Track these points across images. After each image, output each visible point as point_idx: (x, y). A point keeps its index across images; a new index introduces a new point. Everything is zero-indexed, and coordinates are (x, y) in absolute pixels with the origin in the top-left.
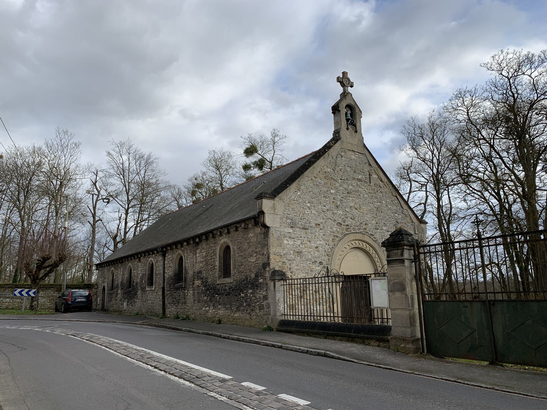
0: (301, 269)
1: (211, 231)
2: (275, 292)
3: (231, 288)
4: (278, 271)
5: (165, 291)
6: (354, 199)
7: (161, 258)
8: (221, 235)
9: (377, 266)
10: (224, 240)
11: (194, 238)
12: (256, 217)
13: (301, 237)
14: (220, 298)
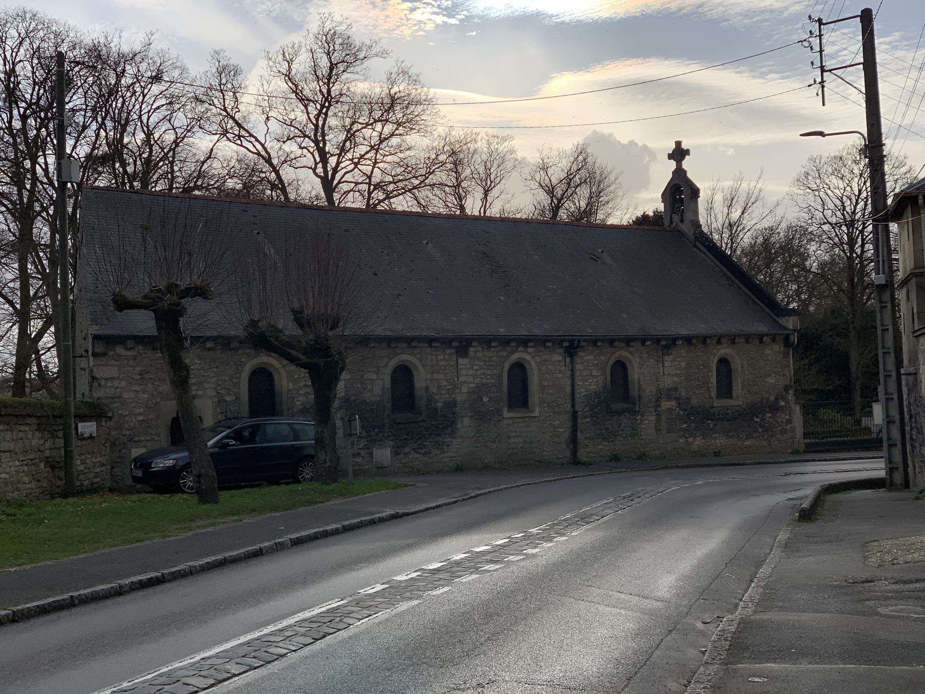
3: (737, 411)
10: (724, 350)
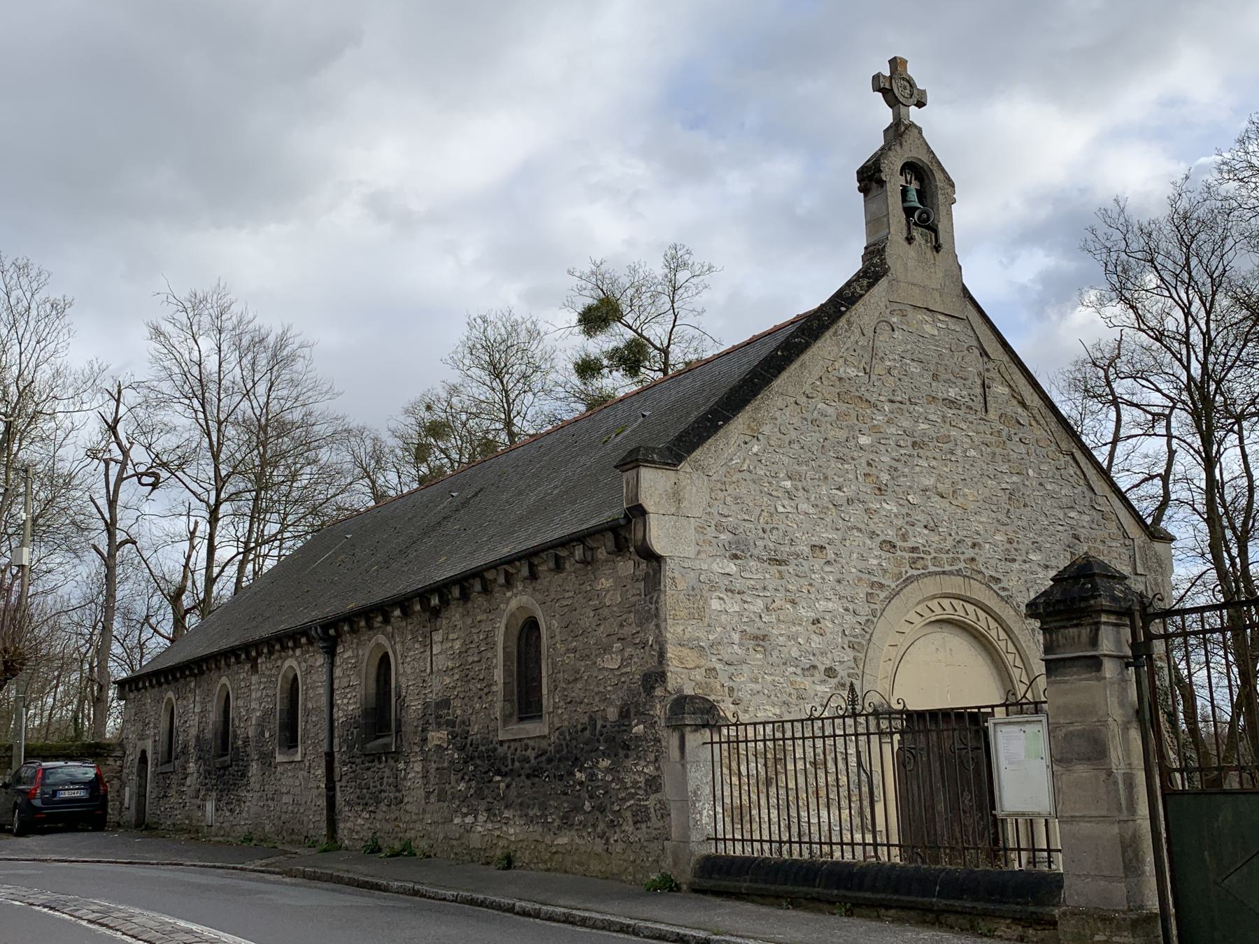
0: (766, 692)
1: (478, 573)
2: (683, 766)
3: (544, 752)
4: (693, 698)
5: (336, 764)
6: (934, 463)
7: (320, 660)
8: (509, 583)
9: (1012, 681)
10: (518, 600)
11: (423, 595)
12: (621, 526)
13: (764, 588)
14: (508, 786)
